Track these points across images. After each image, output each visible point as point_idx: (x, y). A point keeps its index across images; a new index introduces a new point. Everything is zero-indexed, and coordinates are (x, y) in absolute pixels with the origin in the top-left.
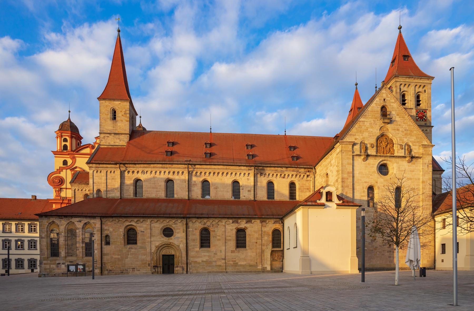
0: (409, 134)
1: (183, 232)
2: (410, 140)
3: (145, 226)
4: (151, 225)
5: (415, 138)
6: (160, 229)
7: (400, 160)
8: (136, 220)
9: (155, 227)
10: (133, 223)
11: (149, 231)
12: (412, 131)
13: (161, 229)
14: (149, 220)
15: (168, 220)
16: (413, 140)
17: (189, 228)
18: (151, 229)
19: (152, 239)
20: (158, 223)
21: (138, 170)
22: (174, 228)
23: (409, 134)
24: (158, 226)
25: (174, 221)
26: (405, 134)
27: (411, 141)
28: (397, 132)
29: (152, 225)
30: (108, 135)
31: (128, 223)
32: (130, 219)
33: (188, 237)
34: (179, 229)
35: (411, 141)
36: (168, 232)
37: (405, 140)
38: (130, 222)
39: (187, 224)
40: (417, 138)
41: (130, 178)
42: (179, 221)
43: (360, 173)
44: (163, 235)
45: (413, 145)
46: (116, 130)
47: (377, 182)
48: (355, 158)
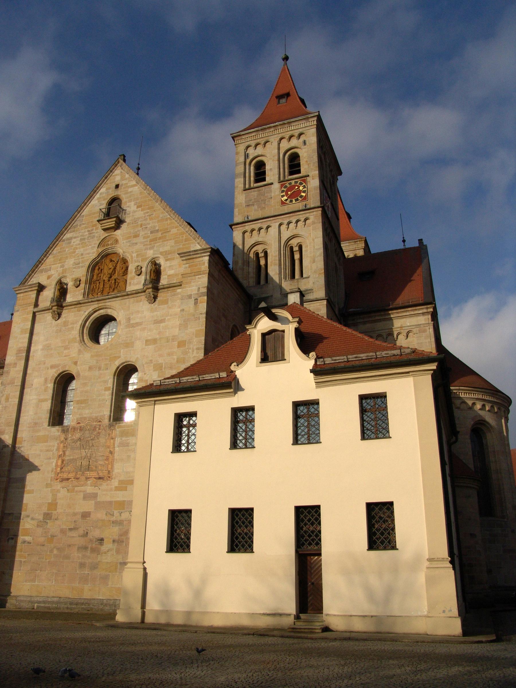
0: (160, 238)
2: (161, 250)
5: (172, 243)
7: (132, 300)
12: (166, 231)
16: (167, 248)
23: (160, 238)
26: (151, 241)
27: (161, 253)
28: (135, 240)
35: (161, 253)
37: (150, 254)
40: (176, 242)
43: (47, 347)
45: (166, 260)
47: (76, 363)
48: (38, 316)
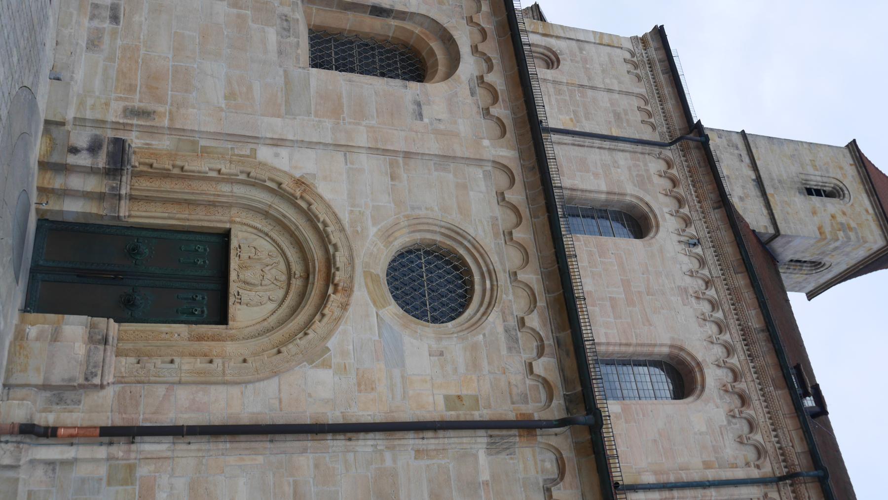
1: (454, 401)
3: (464, 127)
4: (478, 162)
6: (454, 218)
8: (496, 79)
9: (463, 187)
10: (468, 67)
11: (433, 146)
13: (456, 233)
14: (507, 153)
15: (531, 277)
17: (493, 448)
18: (445, 159)
19: (364, 161)
20: (498, 211)
21: (695, 216)
22: (475, 326)
24: (476, 210)
25: (534, 321)
29: (477, 173)
30: (747, 160)
31: (464, 39)
32: (491, 48)
33: (411, 441)
34: (474, 365)
36: (433, 281)
38: (475, 49)
39: (527, 427)
41: (642, 181)
42: (546, 366)
44: (403, 240)
46: (775, 189)
